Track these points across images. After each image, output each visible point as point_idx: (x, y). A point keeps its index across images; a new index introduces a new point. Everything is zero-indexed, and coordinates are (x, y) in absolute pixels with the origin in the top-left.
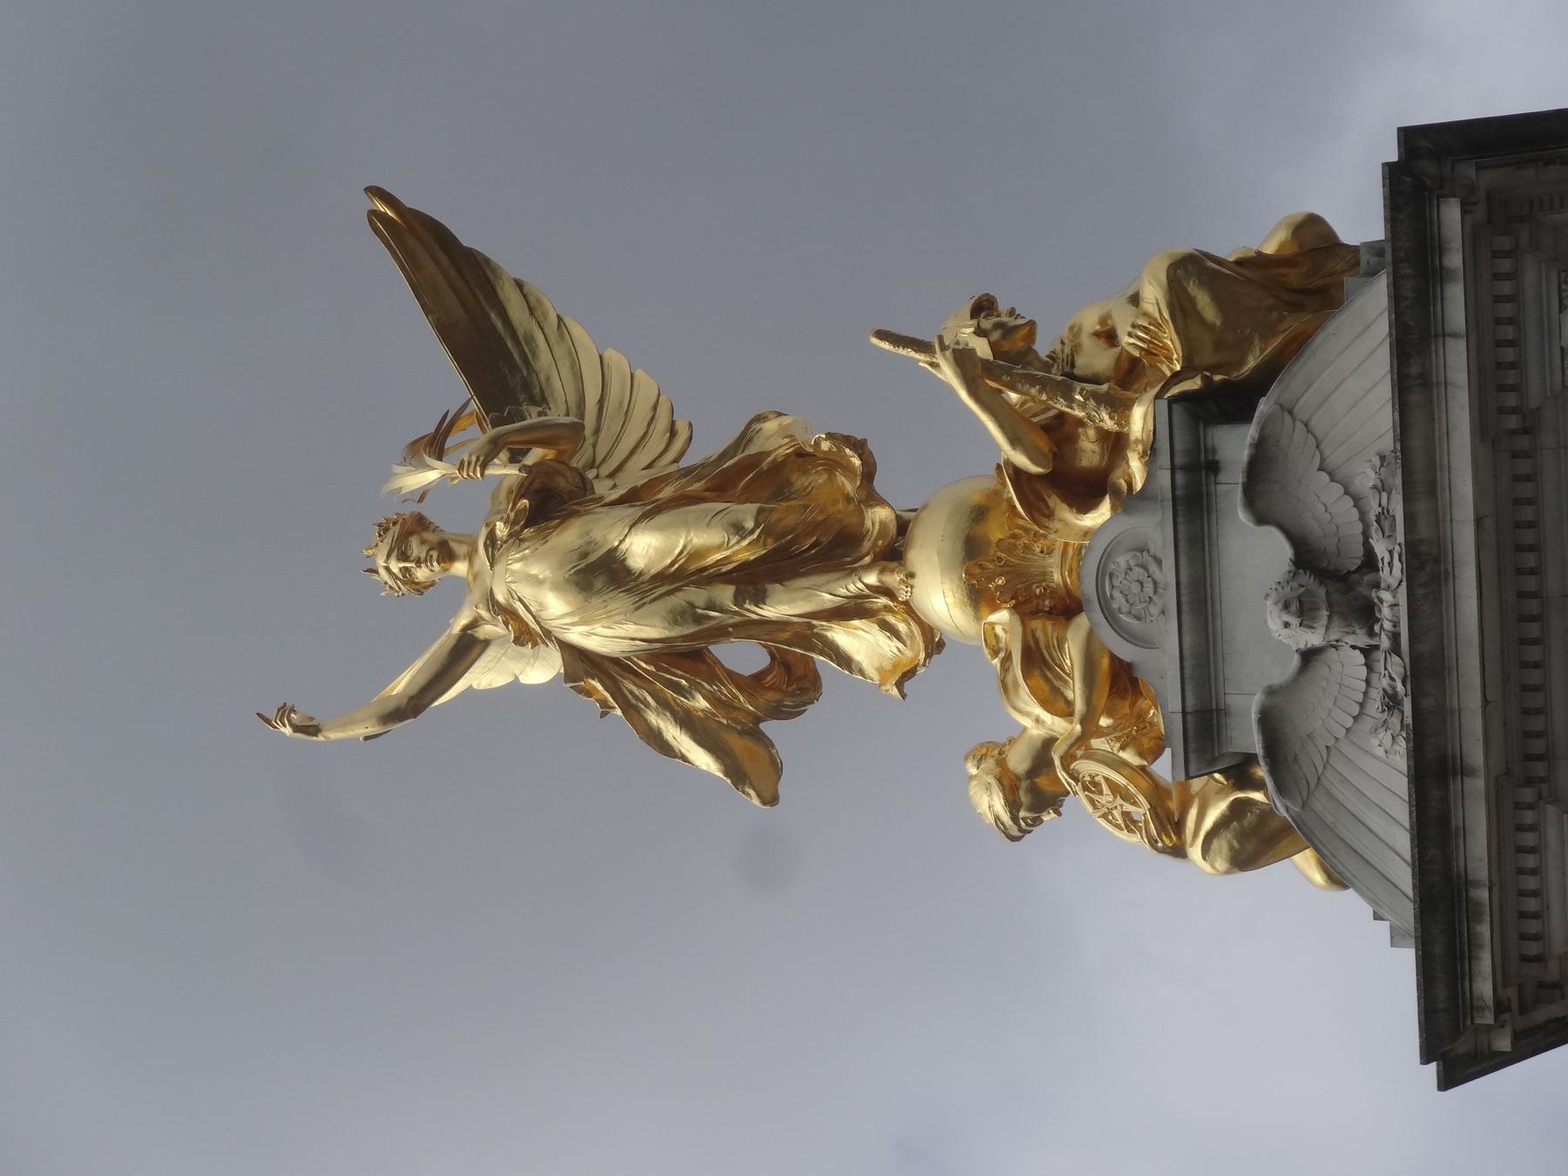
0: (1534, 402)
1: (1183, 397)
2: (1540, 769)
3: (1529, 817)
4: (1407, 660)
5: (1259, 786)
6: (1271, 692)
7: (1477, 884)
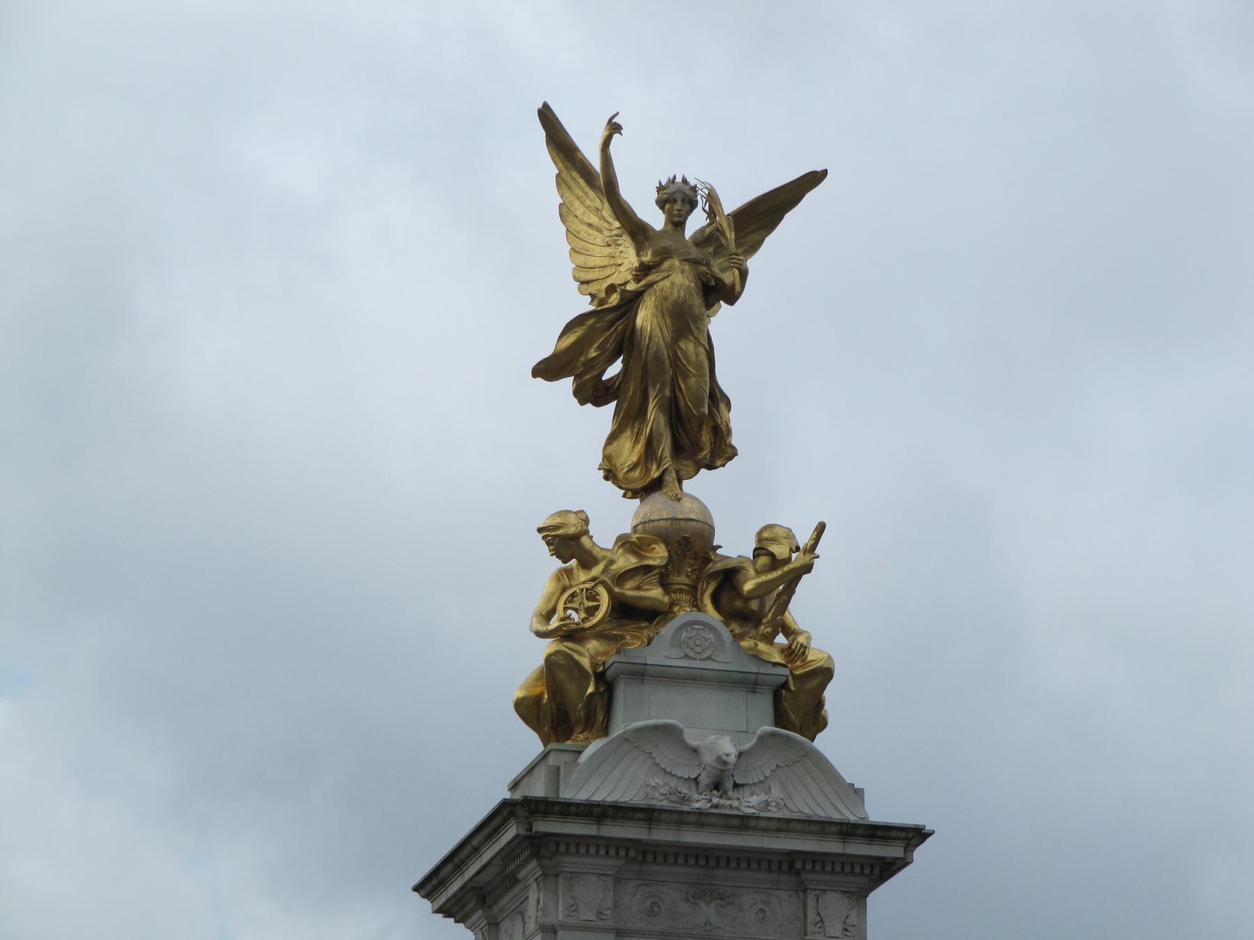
0: (803, 875)
1: (787, 682)
2: (640, 858)
3: (622, 853)
5: (596, 687)
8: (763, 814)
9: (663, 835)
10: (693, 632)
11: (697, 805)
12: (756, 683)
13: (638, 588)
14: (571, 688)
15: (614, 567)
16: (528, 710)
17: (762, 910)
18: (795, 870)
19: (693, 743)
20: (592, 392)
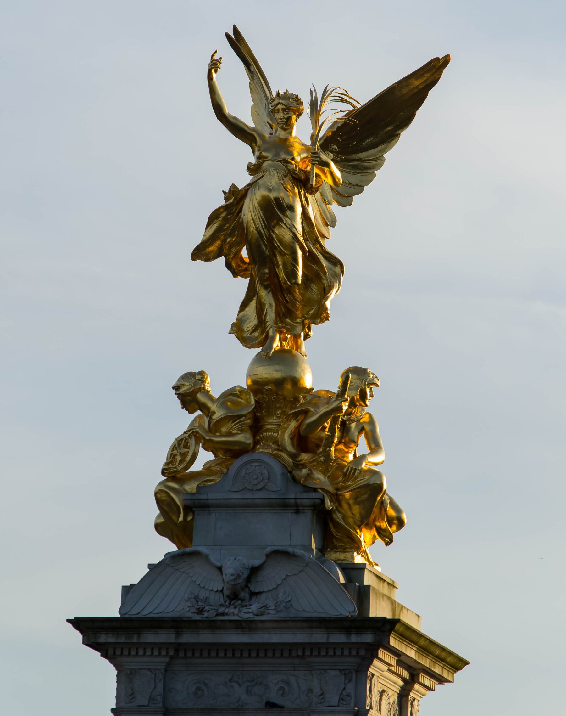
1: (323, 501)
3: (164, 653)
4: (214, 619)
6: (207, 556)
7: (139, 638)
8: (257, 618)
9: (188, 638)
11: (206, 614)
12: (296, 505)
13: (229, 434)
14: (174, 518)
15: (214, 417)
17: (281, 687)
19: (218, 564)
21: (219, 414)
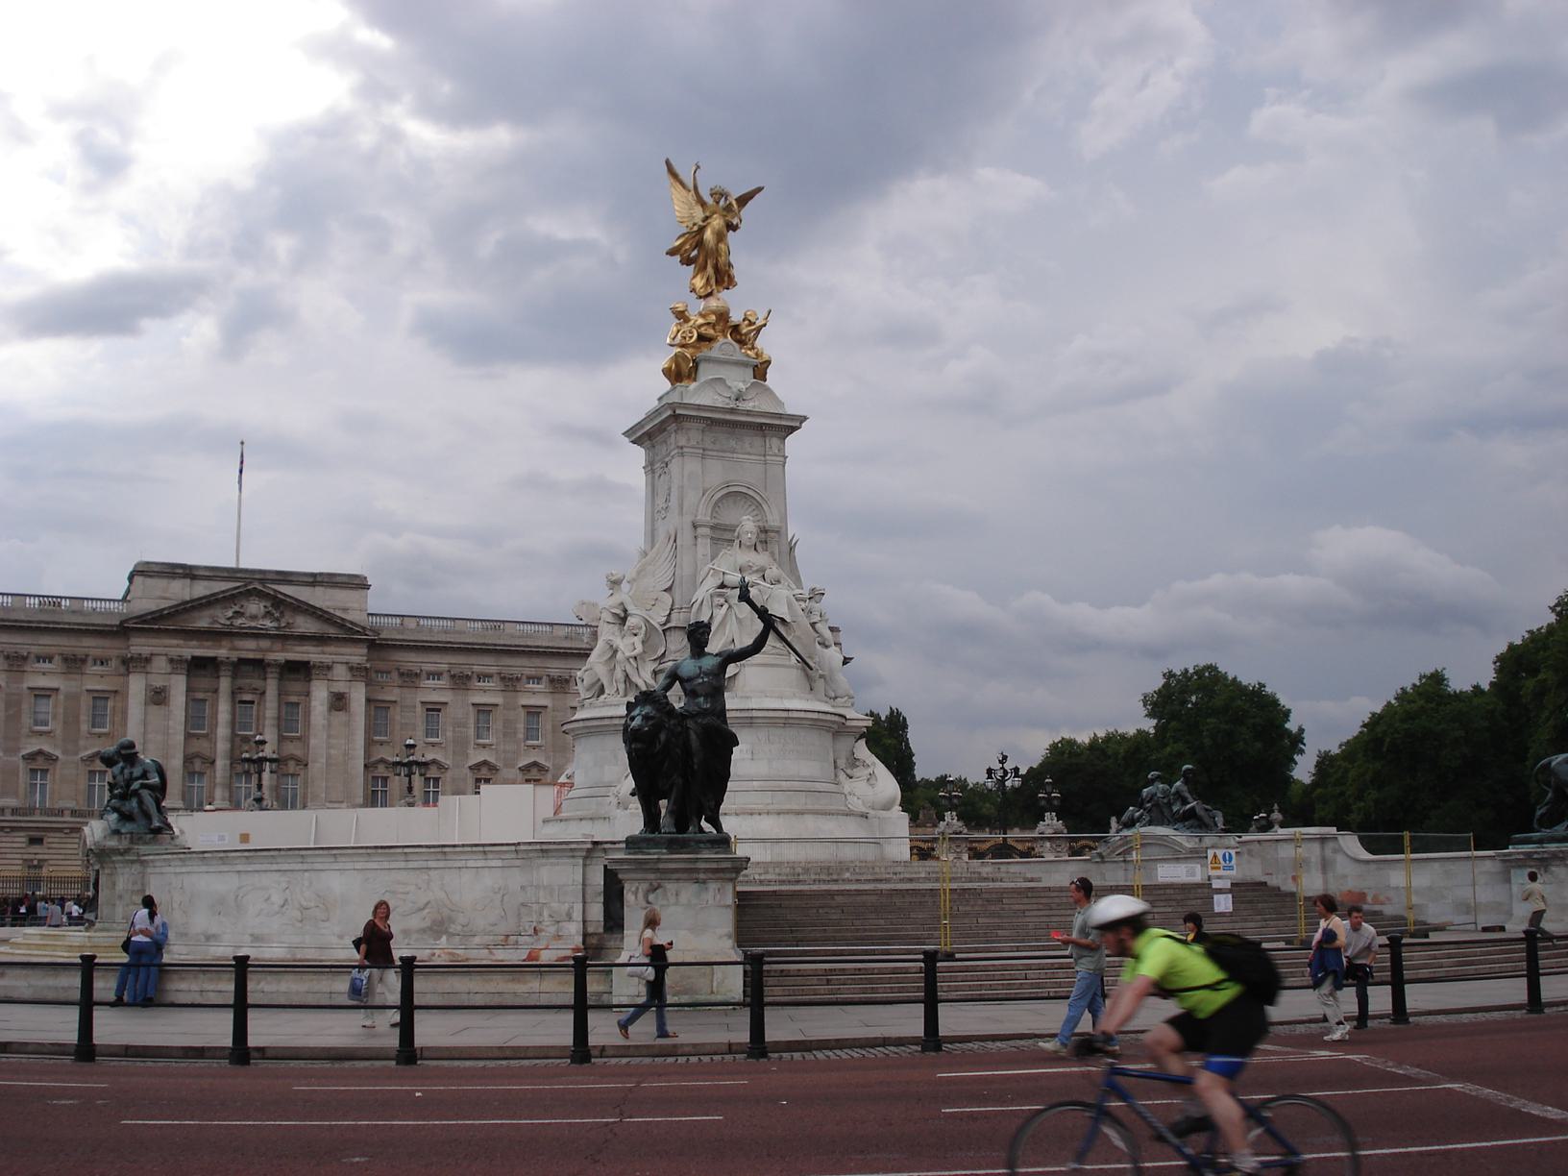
10: (724, 346)
14: (683, 365)
16: (667, 372)
18: (761, 429)
20: (687, 261)
21: (701, 321)
